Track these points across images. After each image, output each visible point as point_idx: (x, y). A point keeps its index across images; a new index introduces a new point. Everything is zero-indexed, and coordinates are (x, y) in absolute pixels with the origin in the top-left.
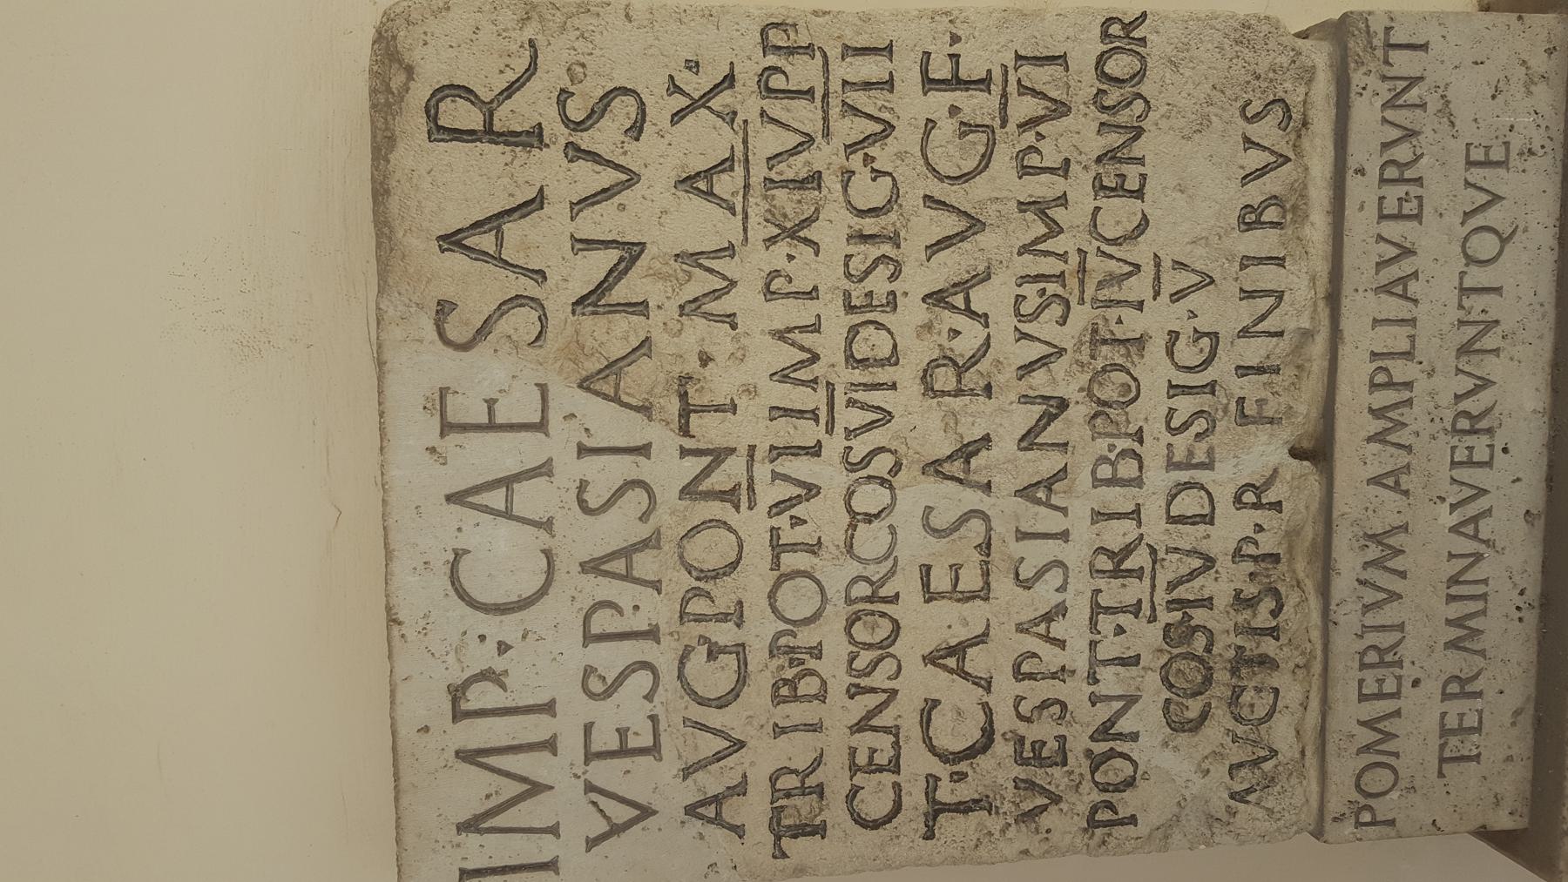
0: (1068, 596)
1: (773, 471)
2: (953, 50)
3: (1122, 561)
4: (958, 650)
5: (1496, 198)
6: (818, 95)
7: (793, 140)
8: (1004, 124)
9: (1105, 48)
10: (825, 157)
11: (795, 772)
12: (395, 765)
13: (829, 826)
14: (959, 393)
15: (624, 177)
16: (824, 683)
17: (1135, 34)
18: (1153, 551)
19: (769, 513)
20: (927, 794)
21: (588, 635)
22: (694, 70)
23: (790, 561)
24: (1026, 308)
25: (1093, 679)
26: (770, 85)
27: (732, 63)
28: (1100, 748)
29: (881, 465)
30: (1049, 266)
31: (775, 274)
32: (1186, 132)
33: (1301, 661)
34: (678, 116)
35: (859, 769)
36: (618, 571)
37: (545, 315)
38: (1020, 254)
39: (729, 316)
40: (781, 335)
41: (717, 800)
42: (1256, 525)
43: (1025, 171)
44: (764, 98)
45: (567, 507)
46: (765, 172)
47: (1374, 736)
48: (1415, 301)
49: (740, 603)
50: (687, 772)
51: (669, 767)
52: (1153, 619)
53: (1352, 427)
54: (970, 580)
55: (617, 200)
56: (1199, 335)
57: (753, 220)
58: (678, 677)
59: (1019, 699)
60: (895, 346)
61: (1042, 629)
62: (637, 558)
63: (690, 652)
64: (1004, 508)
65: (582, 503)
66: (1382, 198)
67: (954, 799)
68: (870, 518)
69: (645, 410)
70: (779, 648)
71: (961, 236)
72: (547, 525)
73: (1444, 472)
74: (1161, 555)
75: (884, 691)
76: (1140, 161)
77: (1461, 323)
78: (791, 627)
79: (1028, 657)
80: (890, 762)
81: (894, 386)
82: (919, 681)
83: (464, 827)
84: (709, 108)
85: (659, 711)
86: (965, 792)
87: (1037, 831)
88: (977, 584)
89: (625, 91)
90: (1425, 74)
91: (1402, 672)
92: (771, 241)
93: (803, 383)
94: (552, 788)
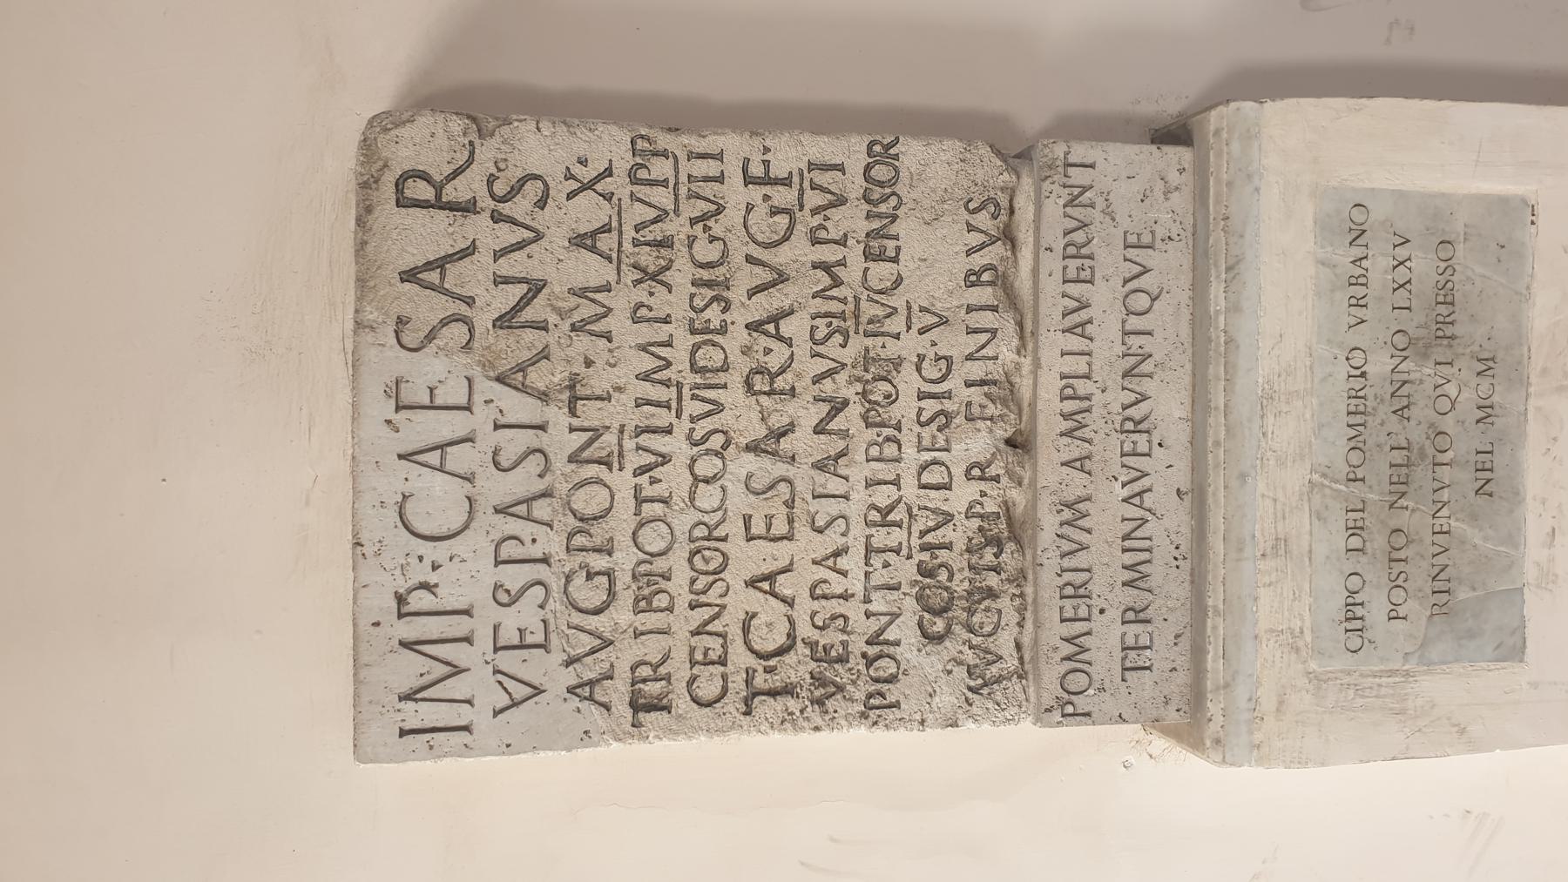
0: (850, 540)
1: (637, 444)
2: (765, 157)
4: (770, 577)
5: (1146, 271)
6: (671, 185)
7: (652, 214)
8: (801, 208)
9: (871, 160)
10: (676, 227)
14: (768, 394)
15: (532, 235)
16: (672, 598)
17: (892, 151)
18: (909, 510)
19: (634, 473)
20: (747, 681)
21: (499, 559)
22: (584, 164)
24: (820, 335)
25: (867, 600)
26: (638, 176)
27: (610, 160)
28: (872, 651)
29: (717, 441)
30: (835, 307)
31: (640, 305)
32: (927, 217)
33: (1017, 592)
34: (571, 196)
36: (521, 514)
37: (473, 328)
38: (813, 297)
40: (643, 348)
41: (591, 683)
42: (981, 491)
43: (816, 242)
44: (632, 183)
45: (486, 465)
46: (633, 233)
47: (1072, 649)
48: (1091, 339)
49: (611, 539)
51: (557, 657)
52: (909, 557)
53: (1049, 425)
54: (780, 527)
55: (527, 250)
56: (938, 358)
57: (623, 267)
58: (564, 592)
59: (813, 614)
60: (726, 357)
61: (830, 562)
62: (535, 504)
63: (574, 573)
64: (803, 476)
65: (496, 464)
66: (1065, 268)
67: (766, 687)
68: (707, 481)
69: (543, 397)
71: (773, 284)
72: (469, 478)
73: (1117, 458)
74: (915, 511)
75: (717, 605)
77: (1124, 356)
78: (648, 557)
79: (821, 582)
80: (720, 657)
81: (725, 386)
82: (742, 600)
84: (594, 190)
85: (550, 617)
86: (776, 681)
87: (827, 712)
90: (1094, 184)
91: (1092, 602)
92: (637, 282)
93: (661, 382)
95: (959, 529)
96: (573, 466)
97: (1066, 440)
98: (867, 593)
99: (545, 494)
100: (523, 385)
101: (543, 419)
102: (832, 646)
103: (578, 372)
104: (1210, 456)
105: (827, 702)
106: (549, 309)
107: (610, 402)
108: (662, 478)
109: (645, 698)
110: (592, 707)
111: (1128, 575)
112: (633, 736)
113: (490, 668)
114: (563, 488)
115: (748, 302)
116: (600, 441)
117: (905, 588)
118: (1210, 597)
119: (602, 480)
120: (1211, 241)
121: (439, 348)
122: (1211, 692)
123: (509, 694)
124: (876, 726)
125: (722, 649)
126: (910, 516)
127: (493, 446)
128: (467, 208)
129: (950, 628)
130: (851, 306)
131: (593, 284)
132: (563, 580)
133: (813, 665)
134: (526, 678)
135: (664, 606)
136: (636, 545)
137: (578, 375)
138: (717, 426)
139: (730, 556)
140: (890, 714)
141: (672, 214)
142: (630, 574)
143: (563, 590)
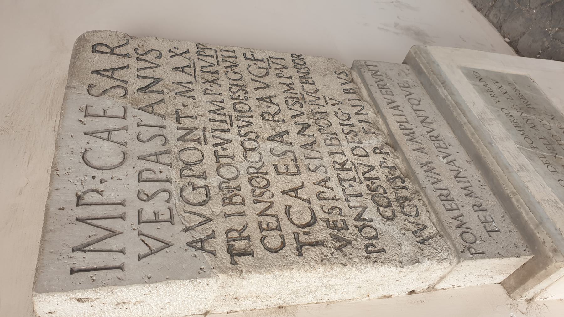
3: (344, 165)
4: (294, 190)
6: (215, 57)
11: (236, 230)
12: (45, 220)
13: (255, 252)
16: (243, 198)
18: (353, 164)
23: (222, 160)
28: (359, 224)
29: (252, 136)
31: (207, 89)
35: (264, 229)
39: (192, 97)
50: (186, 230)
51: (178, 228)
54: (293, 169)
57: (197, 78)
58: (181, 196)
69: (163, 116)
70: (223, 187)
74: (356, 165)
75: (269, 202)
76: (311, 78)
78: (227, 180)
81: (252, 117)
83: (75, 250)
86: (311, 238)
88: (295, 170)
89: (156, 50)
94: (122, 233)
95: (380, 172)
96: (181, 142)
97: (409, 143)
98: (346, 198)
99: (166, 152)
100: (152, 111)
101: (163, 124)
102: (337, 222)
103: (180, 109)
104: (473, 140)
105: (344, 249)
106: (164, 88)
107: (197, 119)
108: (228, 148)
109: (236, 251)
110: (204, 254)
111: (465, 192)
112: (233, 270)
113: (136, 233)
114: (176, 151)
115: (255, 92)
116: (193, 133)
117: (364, 196)
118: (507, 189)
119: (196, 148)
120: (431, 79)
121: (109, 96)
122: (535, 229)
123: (149, 247)
124: (376, 263)
125: (276, 223)
126: (355, 167)
127: (137, 132)
128: (127, 55)
129: (395, 214)
130: (300, 96)
131: (184, 82)
132: (179, 190)
133: (331, 231)
134: (160, 237)
135: (239, 202)
136: (219, 175)
137: (180, 110)
138: (251, 130)
139: (270, 181)
140: (382, 256)
141: (216, 65)
142: (218, 187)
143: (179, 195)
